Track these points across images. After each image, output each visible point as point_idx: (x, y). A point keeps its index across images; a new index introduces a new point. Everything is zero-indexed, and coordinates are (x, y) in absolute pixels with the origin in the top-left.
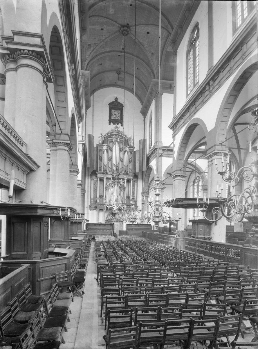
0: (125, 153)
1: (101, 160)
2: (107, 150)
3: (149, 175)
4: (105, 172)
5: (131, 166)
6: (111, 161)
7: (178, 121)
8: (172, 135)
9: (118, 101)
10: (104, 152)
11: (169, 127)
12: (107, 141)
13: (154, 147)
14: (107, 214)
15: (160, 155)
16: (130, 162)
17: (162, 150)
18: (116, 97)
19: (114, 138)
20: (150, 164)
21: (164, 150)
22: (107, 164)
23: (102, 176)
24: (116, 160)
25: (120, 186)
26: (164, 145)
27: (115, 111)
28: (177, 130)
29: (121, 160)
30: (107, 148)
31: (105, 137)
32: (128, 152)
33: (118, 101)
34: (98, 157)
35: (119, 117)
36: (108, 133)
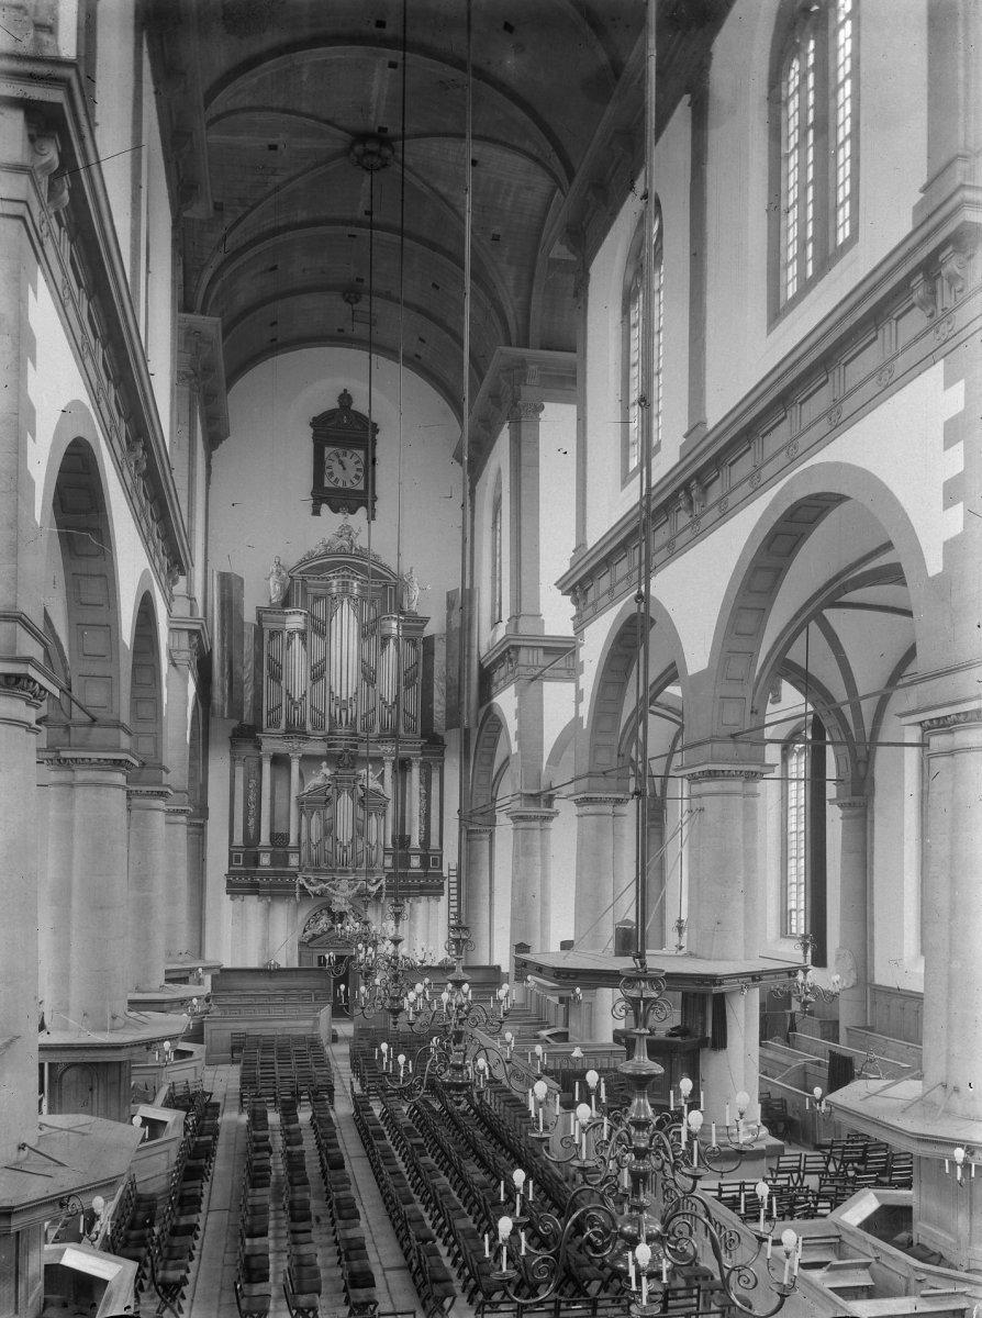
0: (384, 645)
1: (276, 676)
2: (303, 634)
3: (492, 756)
4: (295, 731)
5: (412, 702)
6: (322, 682)
7: (591, 576)
8: (572, 619)
9: (353, 407)
10: (289, 643)
11: (561, 584)
12: (305, 593)
13: (506, 639)
14: (304, 914)
15: (537, 672)
16: (409, 683)
17: (541, 652)
18: (345, 390)
19: (335, 582)
20: (495, 700)
21: (548, 651)
22: (305, 695)
23: (281, 747)
24: (344, 676)
25: (361, 793)
26: (546, 634)
27: (340, 452)
28: (590, 611)
29: (369, 676)
30: (301, 627)
31: (294, 574)
32: (397, 641)
33: (353, 407)
34: (265, 667)
35: (357, 477)
36: (311, 557)
